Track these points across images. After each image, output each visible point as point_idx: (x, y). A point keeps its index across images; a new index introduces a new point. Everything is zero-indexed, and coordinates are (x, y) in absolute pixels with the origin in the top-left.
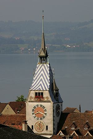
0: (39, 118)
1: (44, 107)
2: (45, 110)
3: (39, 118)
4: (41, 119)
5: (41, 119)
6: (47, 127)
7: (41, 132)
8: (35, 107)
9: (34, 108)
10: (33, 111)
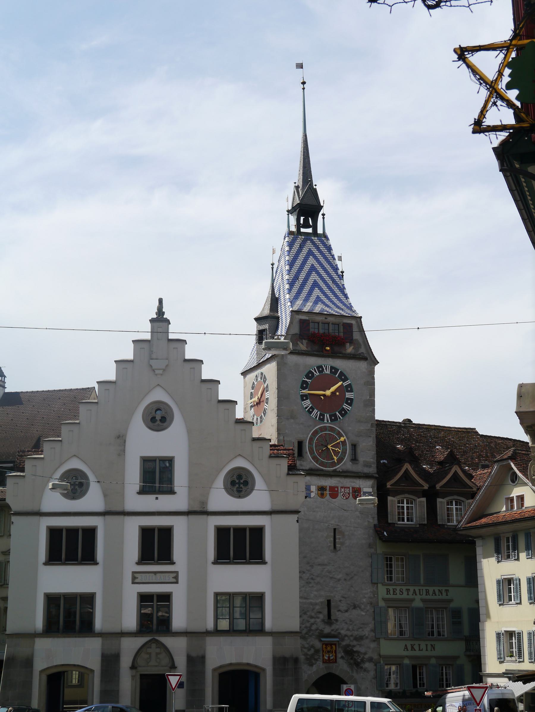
0: (327, 416)
1: (343, 377)
3: (327, 416)
5: (334, 418)
6: (354, 447)
8: (310, 375)
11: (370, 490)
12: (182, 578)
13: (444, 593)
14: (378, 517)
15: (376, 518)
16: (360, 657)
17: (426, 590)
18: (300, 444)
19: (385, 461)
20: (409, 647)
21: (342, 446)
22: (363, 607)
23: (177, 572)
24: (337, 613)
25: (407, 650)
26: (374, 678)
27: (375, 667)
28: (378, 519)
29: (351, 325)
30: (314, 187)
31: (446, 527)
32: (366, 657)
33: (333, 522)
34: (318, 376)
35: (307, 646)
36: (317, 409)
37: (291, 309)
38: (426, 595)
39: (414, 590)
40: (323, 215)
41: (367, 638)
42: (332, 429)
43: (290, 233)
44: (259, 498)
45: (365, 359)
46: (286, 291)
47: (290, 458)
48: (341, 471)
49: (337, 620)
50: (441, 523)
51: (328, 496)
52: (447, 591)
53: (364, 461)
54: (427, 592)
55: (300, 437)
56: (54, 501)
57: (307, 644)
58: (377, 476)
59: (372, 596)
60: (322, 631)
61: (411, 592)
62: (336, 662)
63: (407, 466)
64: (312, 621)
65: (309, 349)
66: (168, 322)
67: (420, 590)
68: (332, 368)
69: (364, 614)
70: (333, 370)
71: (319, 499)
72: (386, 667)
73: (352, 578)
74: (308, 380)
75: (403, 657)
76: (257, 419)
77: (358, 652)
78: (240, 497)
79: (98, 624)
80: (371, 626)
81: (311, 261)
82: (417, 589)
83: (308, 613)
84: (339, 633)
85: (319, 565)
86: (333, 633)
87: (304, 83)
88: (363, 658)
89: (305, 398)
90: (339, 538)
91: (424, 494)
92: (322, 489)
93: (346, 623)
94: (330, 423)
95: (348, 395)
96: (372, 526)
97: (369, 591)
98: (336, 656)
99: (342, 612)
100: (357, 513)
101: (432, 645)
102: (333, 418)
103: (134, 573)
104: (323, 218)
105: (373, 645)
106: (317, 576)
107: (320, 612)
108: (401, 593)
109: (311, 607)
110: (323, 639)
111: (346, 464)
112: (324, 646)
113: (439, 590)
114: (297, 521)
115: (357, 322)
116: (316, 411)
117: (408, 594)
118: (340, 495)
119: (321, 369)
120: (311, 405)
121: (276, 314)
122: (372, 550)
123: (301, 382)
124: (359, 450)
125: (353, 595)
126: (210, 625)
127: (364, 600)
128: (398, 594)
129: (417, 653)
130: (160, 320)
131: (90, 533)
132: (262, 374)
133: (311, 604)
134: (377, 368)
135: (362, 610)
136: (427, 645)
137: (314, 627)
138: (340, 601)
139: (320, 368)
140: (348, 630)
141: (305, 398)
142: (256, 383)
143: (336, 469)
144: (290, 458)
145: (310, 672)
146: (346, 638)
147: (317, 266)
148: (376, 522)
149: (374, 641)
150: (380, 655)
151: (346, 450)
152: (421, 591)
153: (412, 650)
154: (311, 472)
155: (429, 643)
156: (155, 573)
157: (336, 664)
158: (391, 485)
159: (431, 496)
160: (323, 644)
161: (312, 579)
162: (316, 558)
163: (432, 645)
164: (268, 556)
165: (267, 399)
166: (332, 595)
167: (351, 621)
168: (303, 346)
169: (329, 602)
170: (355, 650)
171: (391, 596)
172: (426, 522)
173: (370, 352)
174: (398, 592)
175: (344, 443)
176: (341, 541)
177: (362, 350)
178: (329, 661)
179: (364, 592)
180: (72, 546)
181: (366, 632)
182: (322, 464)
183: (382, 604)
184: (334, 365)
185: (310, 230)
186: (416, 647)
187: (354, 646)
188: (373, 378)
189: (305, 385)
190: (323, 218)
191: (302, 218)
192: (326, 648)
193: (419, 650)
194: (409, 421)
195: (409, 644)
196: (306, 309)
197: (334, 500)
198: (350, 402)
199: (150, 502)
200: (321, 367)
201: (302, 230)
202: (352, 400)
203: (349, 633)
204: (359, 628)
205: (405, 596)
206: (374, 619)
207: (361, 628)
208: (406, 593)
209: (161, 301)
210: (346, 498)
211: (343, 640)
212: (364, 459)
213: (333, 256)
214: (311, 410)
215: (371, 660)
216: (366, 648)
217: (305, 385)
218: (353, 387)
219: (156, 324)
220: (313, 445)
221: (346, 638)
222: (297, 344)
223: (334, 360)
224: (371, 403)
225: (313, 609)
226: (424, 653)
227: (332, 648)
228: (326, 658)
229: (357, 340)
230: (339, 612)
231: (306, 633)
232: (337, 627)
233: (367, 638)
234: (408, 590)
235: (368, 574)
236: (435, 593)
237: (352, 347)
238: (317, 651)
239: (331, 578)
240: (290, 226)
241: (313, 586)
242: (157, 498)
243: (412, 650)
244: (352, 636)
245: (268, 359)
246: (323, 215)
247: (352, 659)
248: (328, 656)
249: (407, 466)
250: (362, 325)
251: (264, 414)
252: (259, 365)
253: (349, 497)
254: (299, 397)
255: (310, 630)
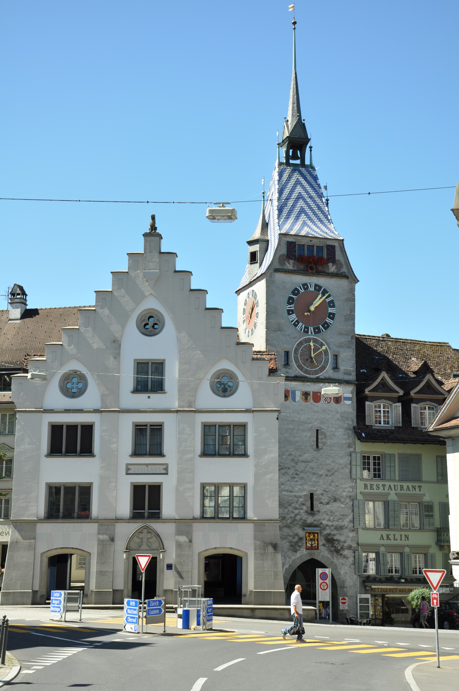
0: (311, 329)
2: (332, 304)
3: (311, 329)
4: (317, 331)
5: (317, 331)
6: (336, 357)
7: (316, 372)
8: (295, 292)
9: (293, 293)
10: (289, 303)
11: (350, 395)
12: (173, 470)
13: (417, 489)
14: (357, 420)
15: (355, 421)
16: (340, 545)
17: (401, 486)
18: (287, 354)
19: (365, 371)
20: (385, 537)
21: (325, 356)
22: (343, 500)
23: (167, 465)
24: (319, 505)
25: (383, 539)
26: (352, 564)
27: (353, 554)
28: (358, 423)
29: (333, 247)
30: (303, 122)
31: (419, 429)
32: (346, 545)
33: (316, 424)
34: (303, 292)
35: (291, 534)
36: (302, 323)
37: (279, 232)
38: (401, 490)
39: (390, 486)
40: (311, 147)
41: (346, 528)
42: (315, 341)
43: (280, 164)
44: (242, 398)
45: (347, 277)
46: (276, 216)
47: (272, 362)
48: (323, 378)
49: (319, 511)
50: (415, 426)
51: (312, 400)
52: (420, 487)
53: (344, 370)
54: (402, 487)
55: (287, 347)
56: (55, 398)
57: (292, 532)
58: (356, 382)
59: (351, 490)
60: (305, 520)
61: (386, 488)
62: (318, 549)
63: (384, 375)
64: (297, 511)
65: (296, 268)
66: (160, 237)
67: (395, 485)
68: (316, 285)
69: (344, 506)
70: (317, 288)
71: (304, 403)
72: (364, 554)
73: (333, 474)
74: (294, 297)
75: (379, 546)
76: (249, 331)
77: (338, 540)
78: (224, 396)
79: (95, 510)
80: (350, 517)
81: (299, 189)
82: (392, 484)
83: (293, 505)
84: (321, 523)
85: (303, 462)
86: (315, 523)
87: (295, 23)
88: (343, 545)
89: (291, 312)
90: (322, 439)
91: (399, 399)
92: (306, 395)
93: (327, 514)
94: (314, 335)
95: (331, 310)
96: (352, 427)
97: (348, 485)
99: (324, 505)
100: (338, 416)
101: (405, 536)
102: (317, 330)
103: (127, 465)
104: (311, 151)
105: (351, 535)
106: (301, 472)
107: (304, 504)
108: (378, 488)
109: (296, 499)
110: (306, 528)
111: (328, 372)
113: (413, 486)
114: (277, 419)
115: (339, 244)
116: (301, 324)
117: (384, 489)
118: (323, 399)
119: (306, 287)
120: (296, 319)
121: (266, 238)
122: (352, 449)
123: (288, 298)
124: (340, 360)
125: (334, 489)
126: (197, 513)
127: (344, 494)
128: (375, 489)
129: (392, 542)
130: (153, 234)
131: (88, 429)
132: (253, 291)
133: (296, 496)
134: (357, 286)
135: (342, 503)
136: (401, 535)
137: (298, 518)
138: (322, 494)
139: (305, 286)
140: (329, 520)
141: (291, 312)
142: (248, 300)
143: (319, 376)
144: (272, 362)
145: (294, 558)
146: (327, 528)
147: (304, 194)
148: (355, 424)
149: (353, 531)
150: (358, 544)
151: (328, 360)
152: (396, 486)
153: (387, 539)
154: (296, 378)
155: (403, 533)
156: (147, 465)
158: (369, 391)
159: (406, 402)
160: (306, 533)
161: (296, 474)
162: (300, 456)
163: (405, 536)
164: (250, 450)
165: (257, 313)
166: (314, 489)
167: (331, 512)
168: (290, 265)
169: (312, 495)
170: (335, 538)
171: (369, 491)
172: (401, 425)
173: (351, 270)
174: (375, 487)
175: (326, 352)
176: (323, 440)
177: (344, 270)
178: (312, 548)
179: (344, 486)
180: (71, 440)
181: (346, 522)
182: (306, 372)
183: (360, 497)
184: (318, 283)
185: (298, 162)
186: (391, 537)
187: (334, 535)
188: (354, 296)
189: (291, 301)
190: (311, 151)
191: (291, 151)
192: (309, 536)
193: (394, 540)
194: (388, 335)
195: (385, 533)
196: (293, 233)
197: (317, 404)
198: (332, 316)
199: (143, 400)
200: (306, 284)
201: (291, 161)
202: (334, 314)
203: (330, 523)
204: (339, 519)
205: (381, 490)
206: (353, 511)
207: (341, 519)
208: (383, 488)
209: (153, 218)
210: (328, 403)
211: (324, 529)
212: (344, 368)
213: (319, 185)
214: (296, 323)
215: (350, 547)
216: (346, 538)
217: (291, 301)
218: (336, 303)
219: (149, 238)
220: (298, 354)
221: (327, 528)
222: (285, 264)
223: (318, 278)
224: (351, 318)
225: (297, 501)
226: (399, 542)
227: (314, 536)
228: (309, 546)
229: (339, 260)
230: (321, 504)
231: (291, 523)
232: (320, 517)
233: (346, 528)
234: (384, 486)
235: (348, 470)
236: (409, 489)
237: (335, 267)
238: (301, 539)
239: (314, 474)
240: (280, 157)
241: (297, 481)
242: (149, 397)
243: (387, 539)
244: (332, 526)
245: (258, 278)
246: (311, 147)
247: (332, 546)
248: (310, 543)
249: (384, 375)
250: (344, 247)
251: (255, 327)
252: (251, 284)
253: (330, 401)
254: (286, 312)
255: (294, 520)
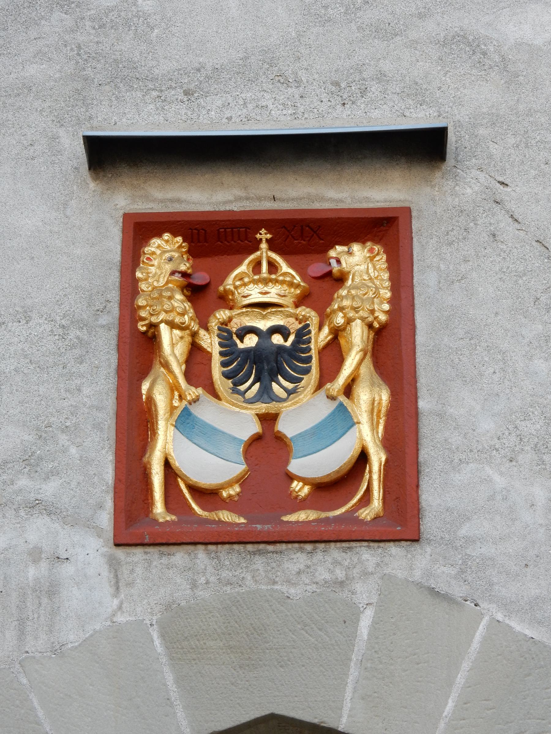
62: (402, 522)
98: (402, 429)
112: (164, 255)
157: (396, 559)
160: (141, 230)
178: (266, 508)
227: (324, 287)
248: (238, 420)
